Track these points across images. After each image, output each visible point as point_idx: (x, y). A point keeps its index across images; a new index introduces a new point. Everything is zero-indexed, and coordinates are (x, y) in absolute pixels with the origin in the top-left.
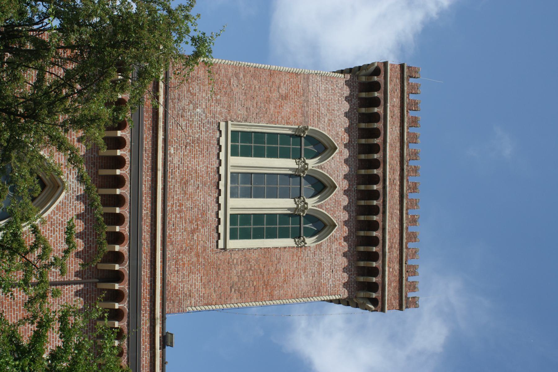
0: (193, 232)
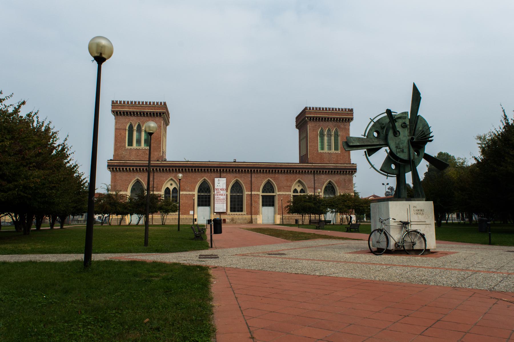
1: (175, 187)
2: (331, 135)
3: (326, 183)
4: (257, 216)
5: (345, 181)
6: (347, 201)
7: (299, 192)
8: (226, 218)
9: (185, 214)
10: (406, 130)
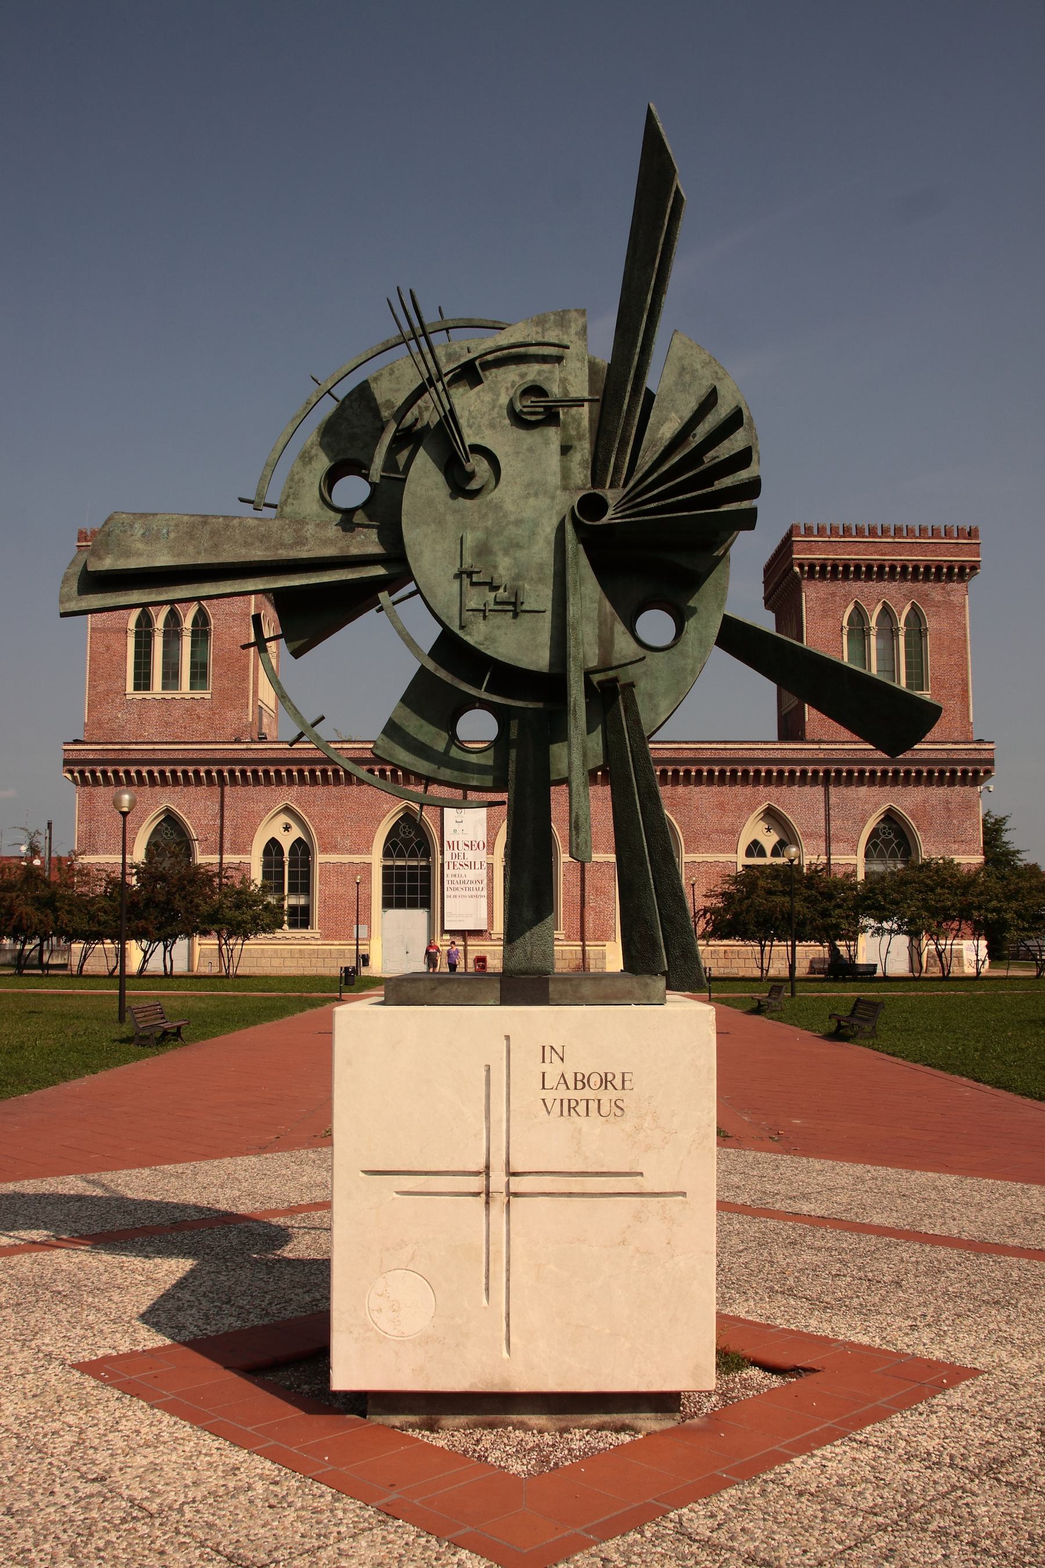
0: (199, 718)
1: (300, 838)
2: (894, 633)
3: (875, 816)
4: (605, 946)
5: (949, 810)
6: (939, 890)
7: (768, 852)
8: (488, 951)
9: (336, 939)
10: (547, 442)
